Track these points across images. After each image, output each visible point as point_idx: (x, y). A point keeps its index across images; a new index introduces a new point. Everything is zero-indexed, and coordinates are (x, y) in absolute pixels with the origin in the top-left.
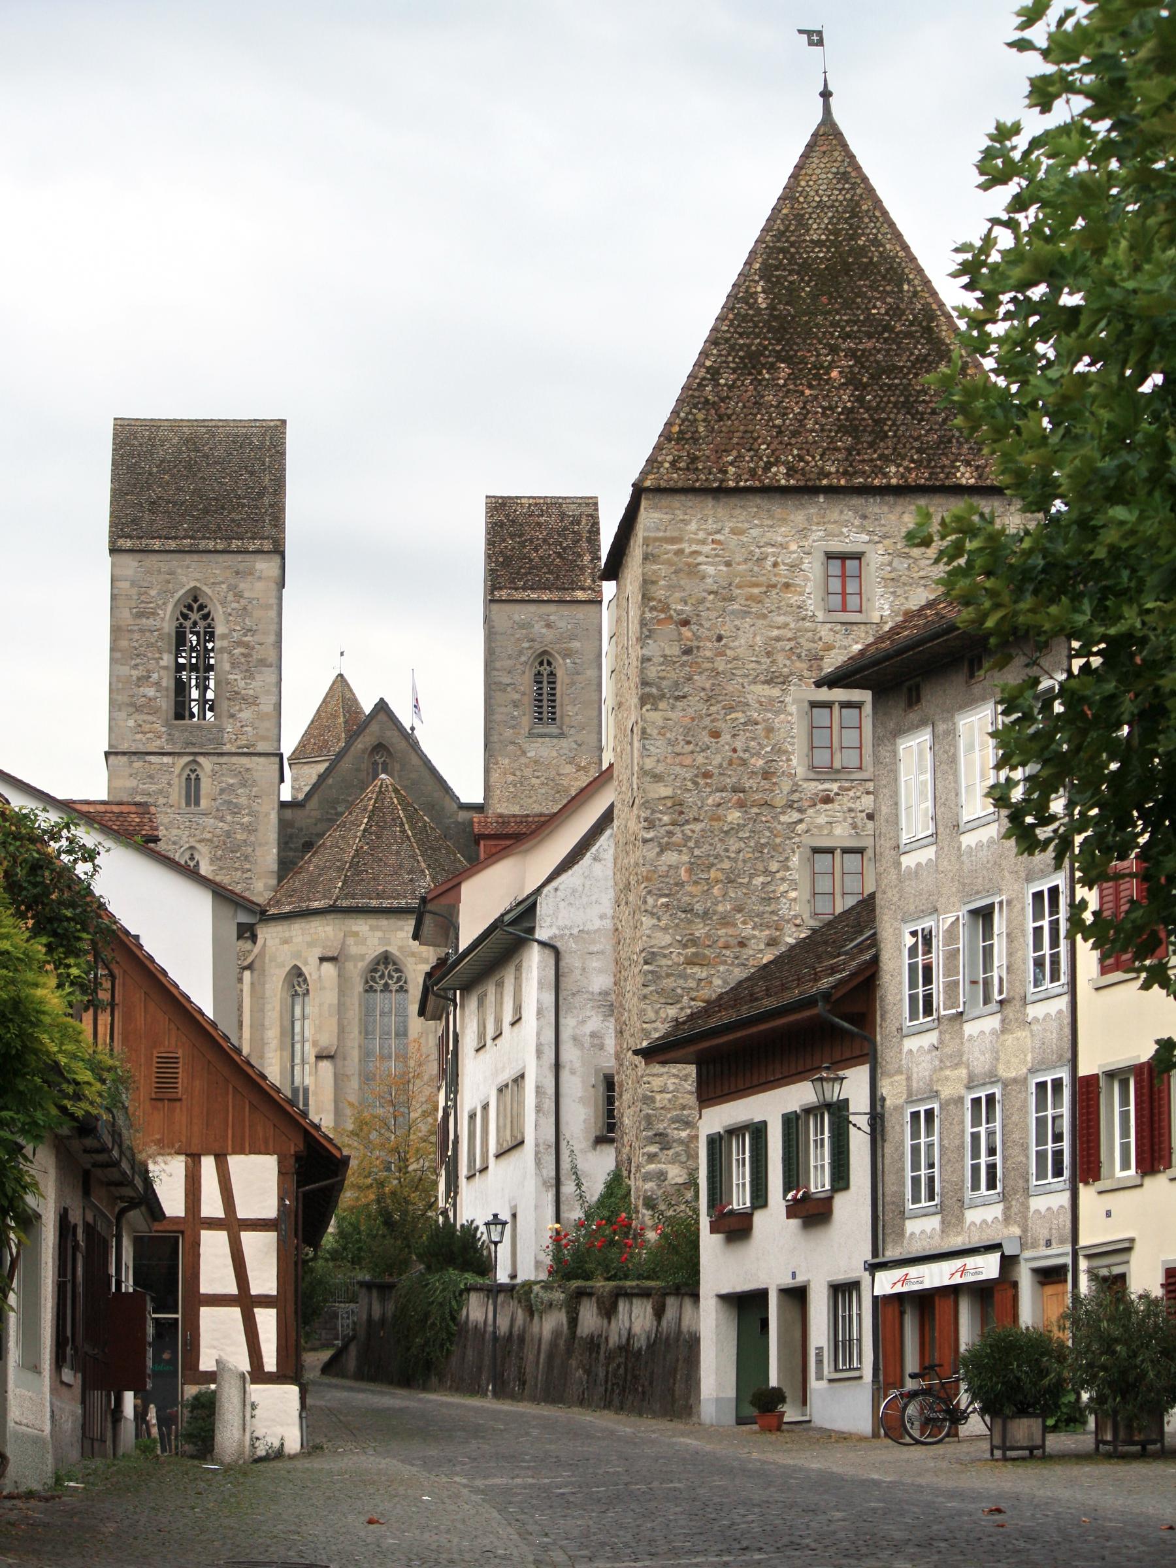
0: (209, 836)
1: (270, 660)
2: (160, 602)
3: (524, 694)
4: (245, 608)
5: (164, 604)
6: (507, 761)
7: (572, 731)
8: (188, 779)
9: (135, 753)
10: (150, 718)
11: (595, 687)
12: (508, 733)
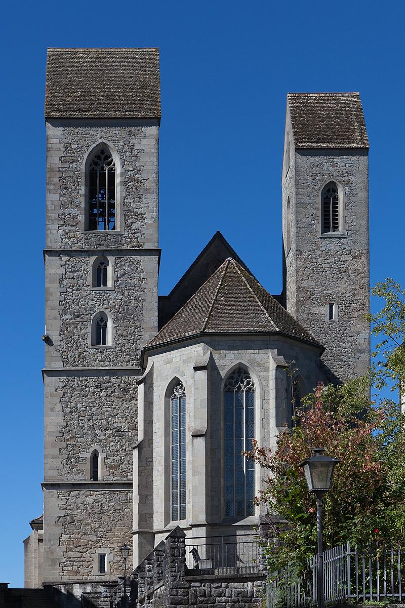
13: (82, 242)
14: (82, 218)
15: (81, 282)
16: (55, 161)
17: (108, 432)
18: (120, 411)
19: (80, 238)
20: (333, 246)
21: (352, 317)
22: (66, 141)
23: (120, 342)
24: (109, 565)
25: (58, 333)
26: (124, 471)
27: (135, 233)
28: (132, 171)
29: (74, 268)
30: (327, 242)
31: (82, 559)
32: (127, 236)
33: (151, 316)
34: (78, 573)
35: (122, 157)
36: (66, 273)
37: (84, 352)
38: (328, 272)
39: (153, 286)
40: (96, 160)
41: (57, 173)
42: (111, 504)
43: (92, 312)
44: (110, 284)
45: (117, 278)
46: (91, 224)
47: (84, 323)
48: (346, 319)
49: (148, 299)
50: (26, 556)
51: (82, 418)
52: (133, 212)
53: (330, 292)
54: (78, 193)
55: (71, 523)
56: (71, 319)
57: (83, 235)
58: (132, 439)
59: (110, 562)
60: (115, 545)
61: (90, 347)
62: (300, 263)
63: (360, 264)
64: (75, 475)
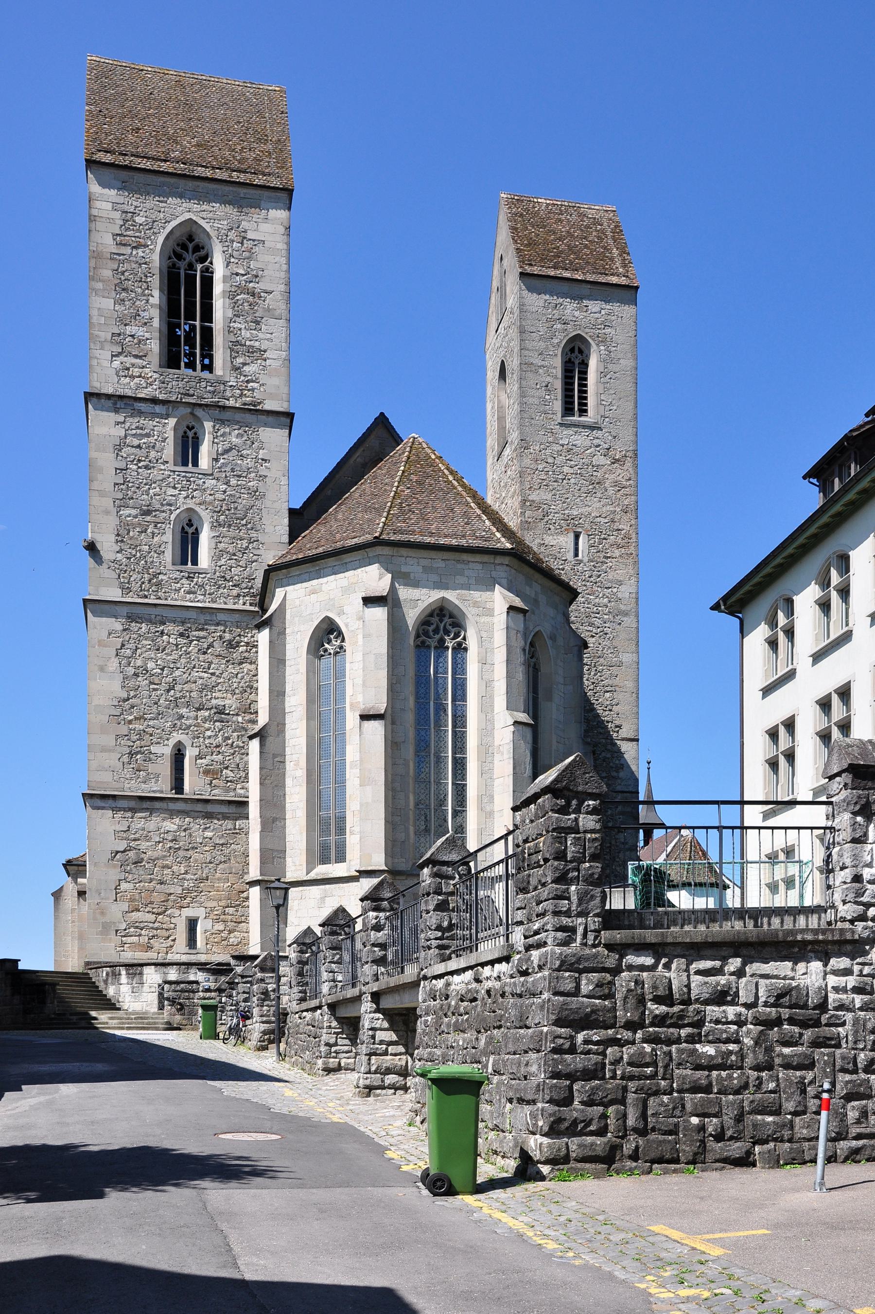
13: (155, 387)
14: (154, 346)
15: (153, 454)
16: (106, 241)
17: (200, 713)
18: (222, 680)
19: (151, 380)
20: (581, 439)
21: (609, 557)
22: (126, 208)
23: (223, 562)
24: (204, 936)
25: (113, 538)
26: (231, 781)
27: (248, 382)
28: (243, 275)
29: (142, 429)
30: (572, 433)
31: (156, 925)
32: (234, 384)
33: (280, 526)
34: (149, 948)
35: (226, 249)
36: (126, 437)
37: (159, 574)
38: (573, 481)
39: (280, 473)
42: (209, 834)
43: (173, 508)
44: (204, 462)
45: (218, 454)
46: (171, 360)
47: (159, 525)
48: (600, 559)
49: (271, 496)
50: (56, 917)
51: (156, 687)
52: (245, 345)
53: (575, 513)
54: (147, 301)
55: (136, 863)
56: (135, 517)
57: (156, 376)
58: (243, 728)
59: (206, 931)
60: (214, 904)
61: (170, 566)
62: (527, 462)
63: (622, 473)
64: (145, 782)
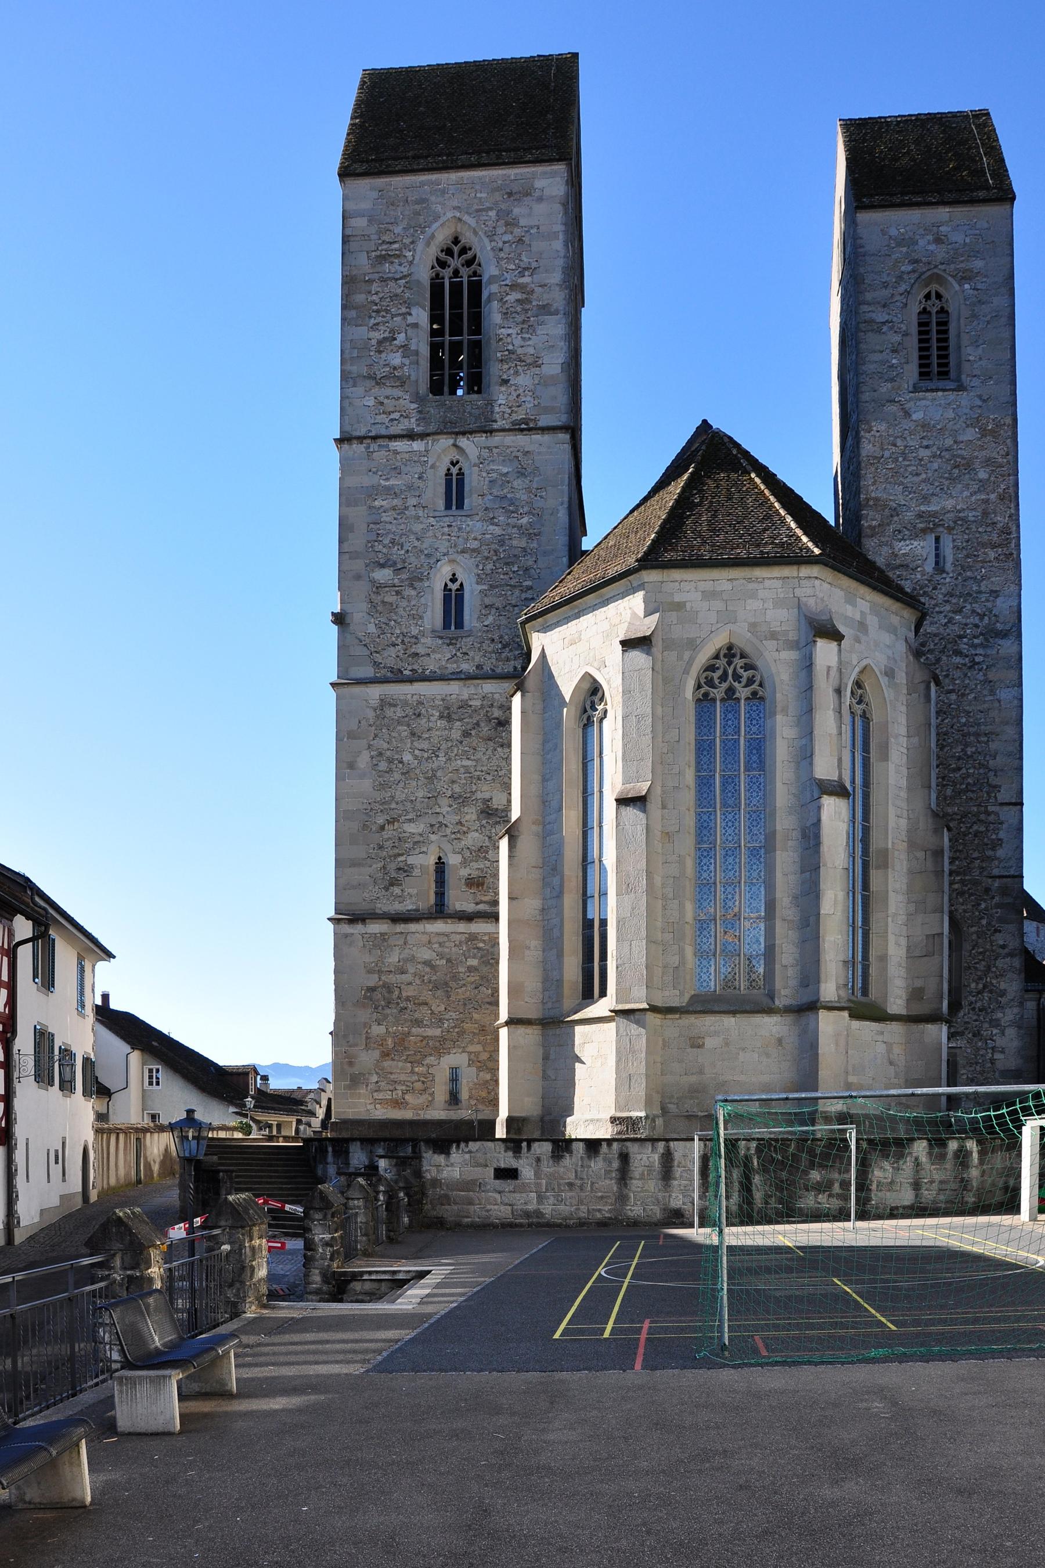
0: (475, 545)
1: (555, 305)
2: (407, 241)
3: (906, 334)
4: (520, 241)
5: (413, 242)
6: (883, 427)
7: (976, 382)
8: (448, 474)
9: (375, 438)
10: (397, 392)
11: (1004, 320)
12: (885, 388)
40: (443, 256)
41: (363, 284)
